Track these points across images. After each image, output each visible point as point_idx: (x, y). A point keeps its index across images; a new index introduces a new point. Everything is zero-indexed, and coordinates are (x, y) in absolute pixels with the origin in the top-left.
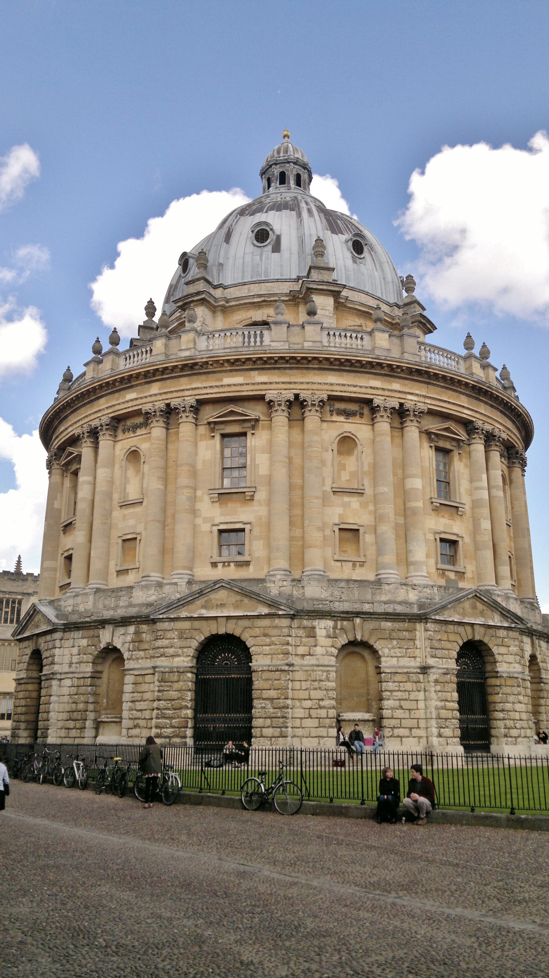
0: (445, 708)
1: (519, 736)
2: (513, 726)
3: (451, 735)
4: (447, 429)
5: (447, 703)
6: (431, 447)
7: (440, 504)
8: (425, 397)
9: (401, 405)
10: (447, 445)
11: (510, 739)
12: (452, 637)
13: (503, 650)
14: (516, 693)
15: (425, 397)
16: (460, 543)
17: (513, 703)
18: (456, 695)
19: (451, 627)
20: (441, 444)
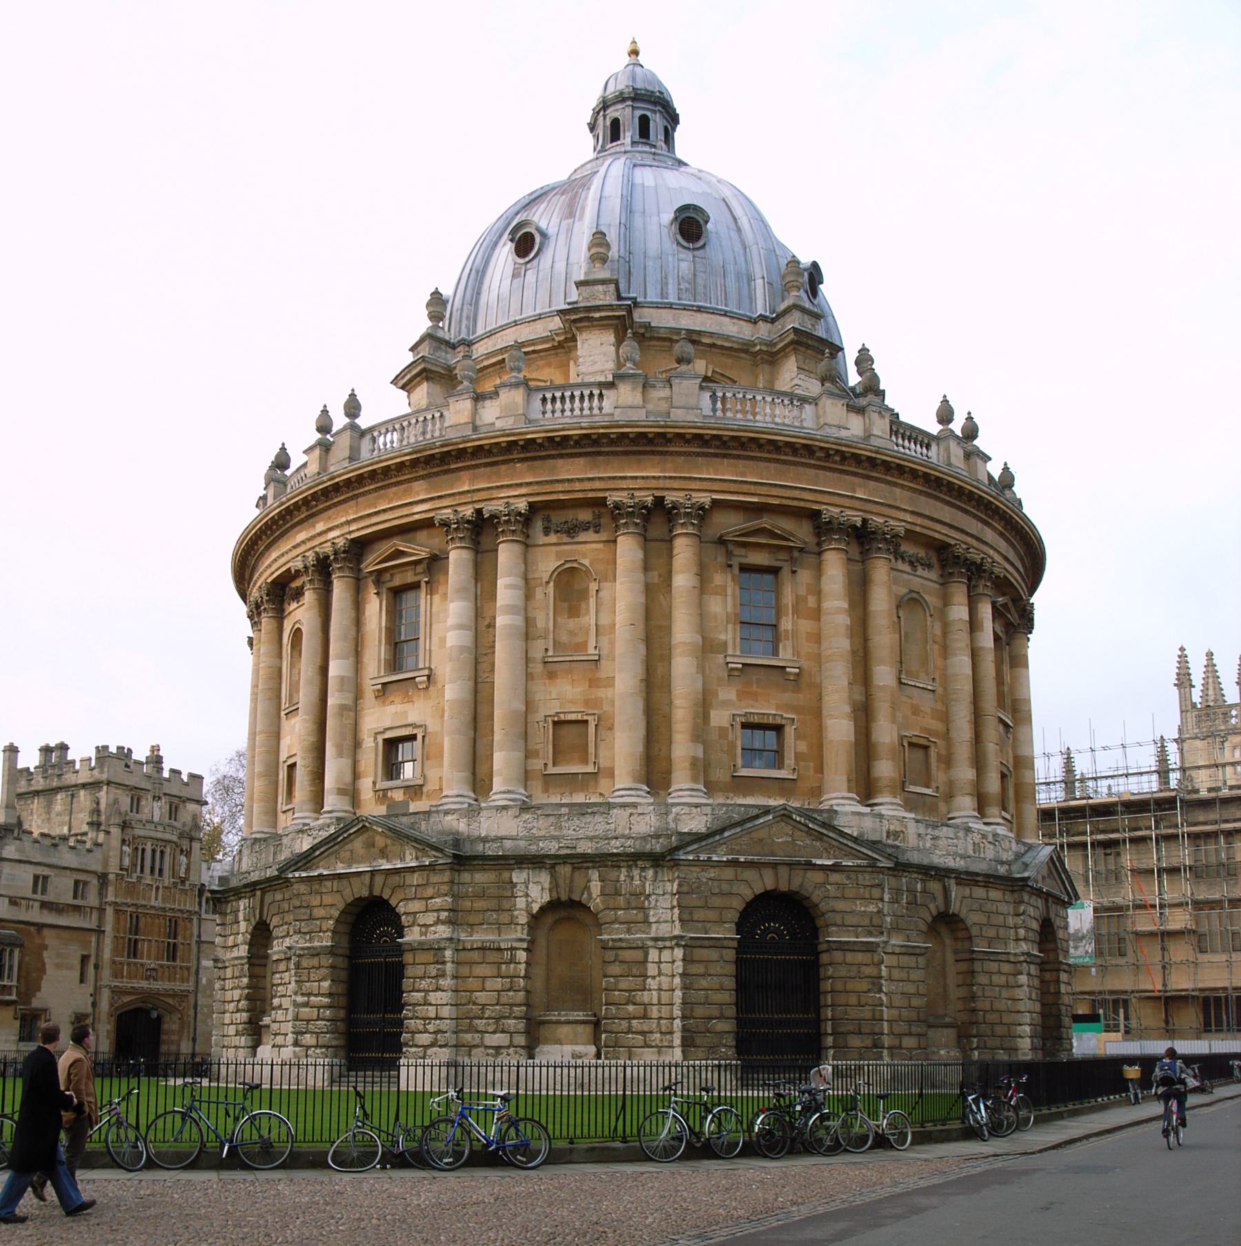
0: (306, 1005)
1: (433, 1045)
2: (421, 1027)
3: (314, 1042)
4: (400, 554)
5: (312, 998)
6: (377, 594)
7: (384, 684)
8: (348, 523)
9: (317, 553)
10: (410, 578)
11: (413, 1050)
12: (328, 899)
13: (415, 906)
14: (434, 973)
15: (348, 523)
16: (419, 737)
17: (427, 991)
18: (326, 984)
19: (329, 884)
20: (397, 581)
